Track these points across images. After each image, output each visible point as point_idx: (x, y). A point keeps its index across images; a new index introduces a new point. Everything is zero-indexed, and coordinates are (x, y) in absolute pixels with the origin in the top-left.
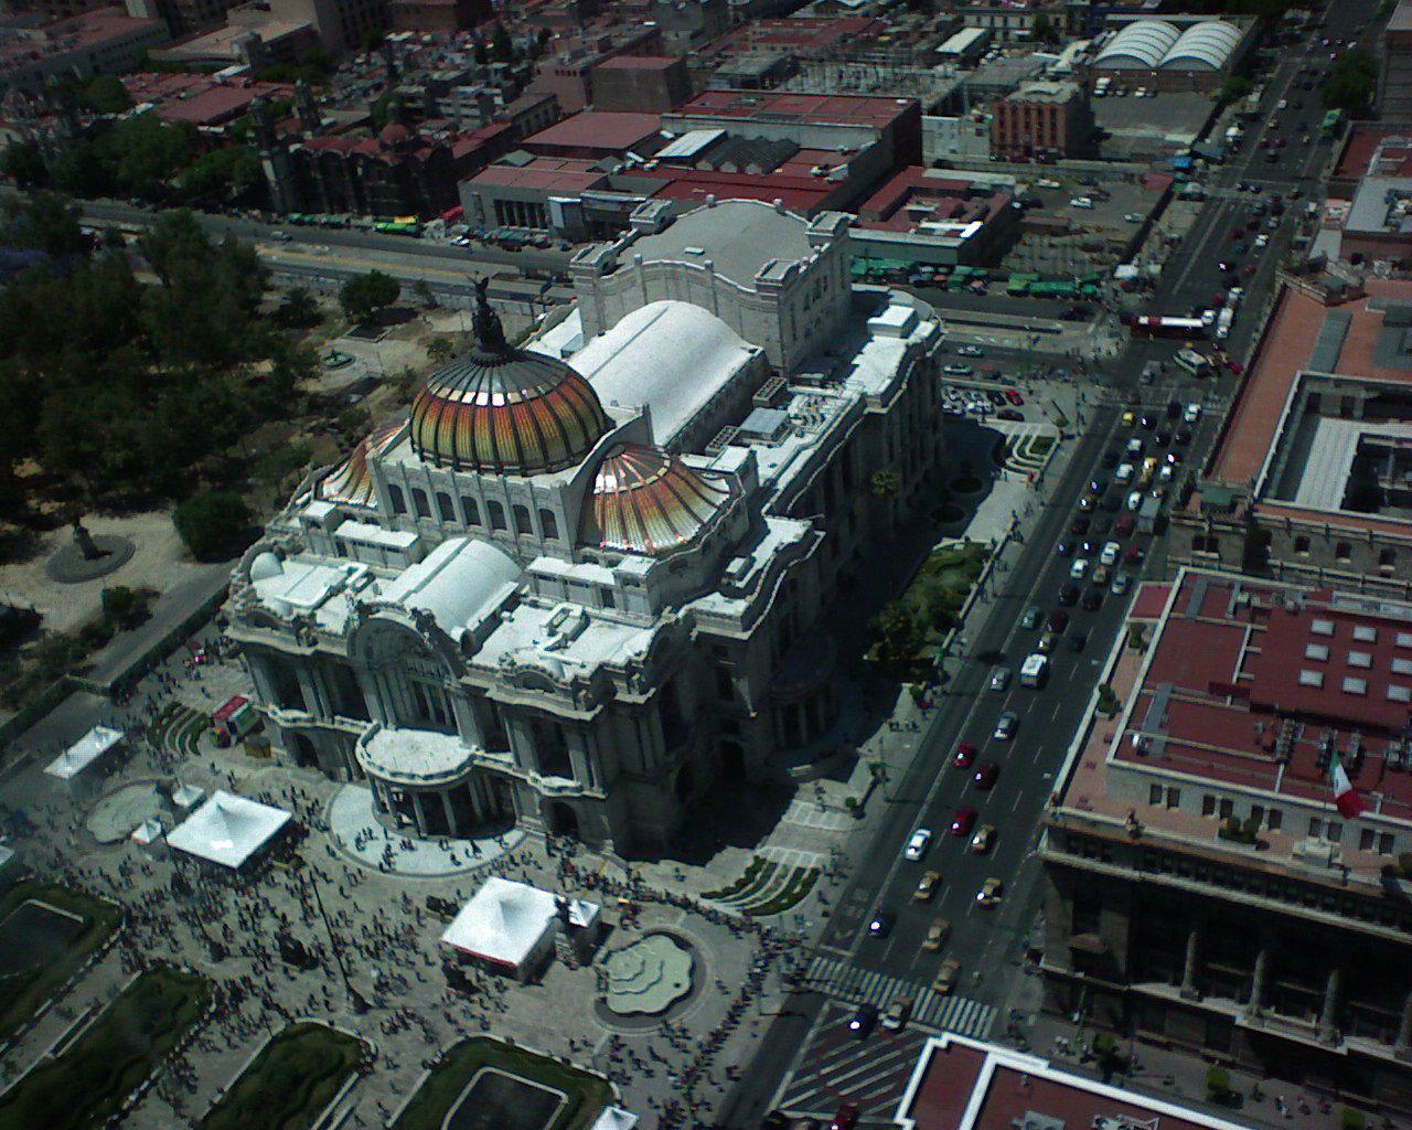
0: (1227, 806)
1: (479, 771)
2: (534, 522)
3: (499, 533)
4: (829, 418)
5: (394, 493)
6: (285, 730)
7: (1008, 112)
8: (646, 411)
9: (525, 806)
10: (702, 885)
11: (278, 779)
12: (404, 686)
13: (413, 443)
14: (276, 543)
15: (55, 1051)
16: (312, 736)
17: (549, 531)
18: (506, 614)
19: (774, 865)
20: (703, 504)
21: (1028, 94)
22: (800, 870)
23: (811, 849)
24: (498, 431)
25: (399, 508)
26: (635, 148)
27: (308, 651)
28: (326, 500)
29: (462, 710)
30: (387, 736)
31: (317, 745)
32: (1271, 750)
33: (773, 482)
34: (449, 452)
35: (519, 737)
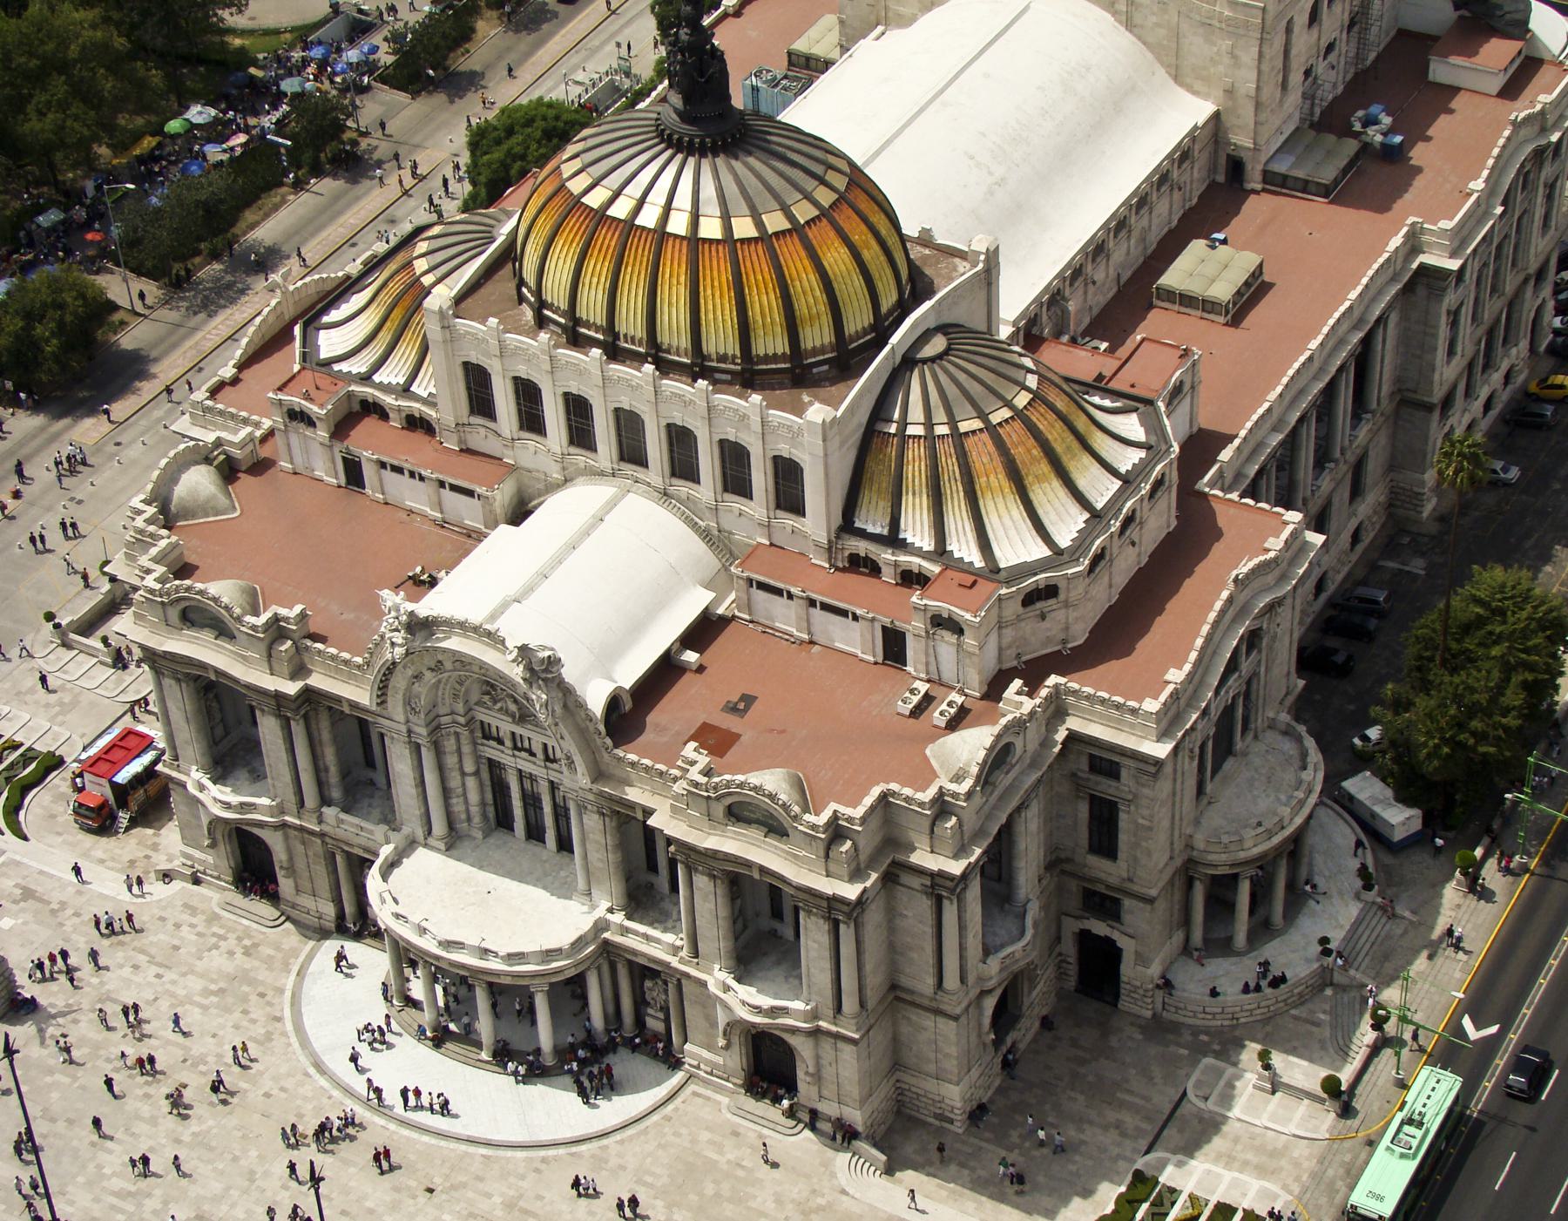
1: (609, 953)
2: (761, 478)
3: (682, 488)
6: (216, 822)
8: (992, 258)
11: (193, 911)
12: (469, 767)
14: (219, 443)
17: (789, 496)
18: (691, 657)
20: (1096, 468)
23: (1244, 1166)
24: (706, 293)
25: (481, 403)
27: (291, 688)
29: (590, 831)
34: (599, 318)
35: (705, 901)
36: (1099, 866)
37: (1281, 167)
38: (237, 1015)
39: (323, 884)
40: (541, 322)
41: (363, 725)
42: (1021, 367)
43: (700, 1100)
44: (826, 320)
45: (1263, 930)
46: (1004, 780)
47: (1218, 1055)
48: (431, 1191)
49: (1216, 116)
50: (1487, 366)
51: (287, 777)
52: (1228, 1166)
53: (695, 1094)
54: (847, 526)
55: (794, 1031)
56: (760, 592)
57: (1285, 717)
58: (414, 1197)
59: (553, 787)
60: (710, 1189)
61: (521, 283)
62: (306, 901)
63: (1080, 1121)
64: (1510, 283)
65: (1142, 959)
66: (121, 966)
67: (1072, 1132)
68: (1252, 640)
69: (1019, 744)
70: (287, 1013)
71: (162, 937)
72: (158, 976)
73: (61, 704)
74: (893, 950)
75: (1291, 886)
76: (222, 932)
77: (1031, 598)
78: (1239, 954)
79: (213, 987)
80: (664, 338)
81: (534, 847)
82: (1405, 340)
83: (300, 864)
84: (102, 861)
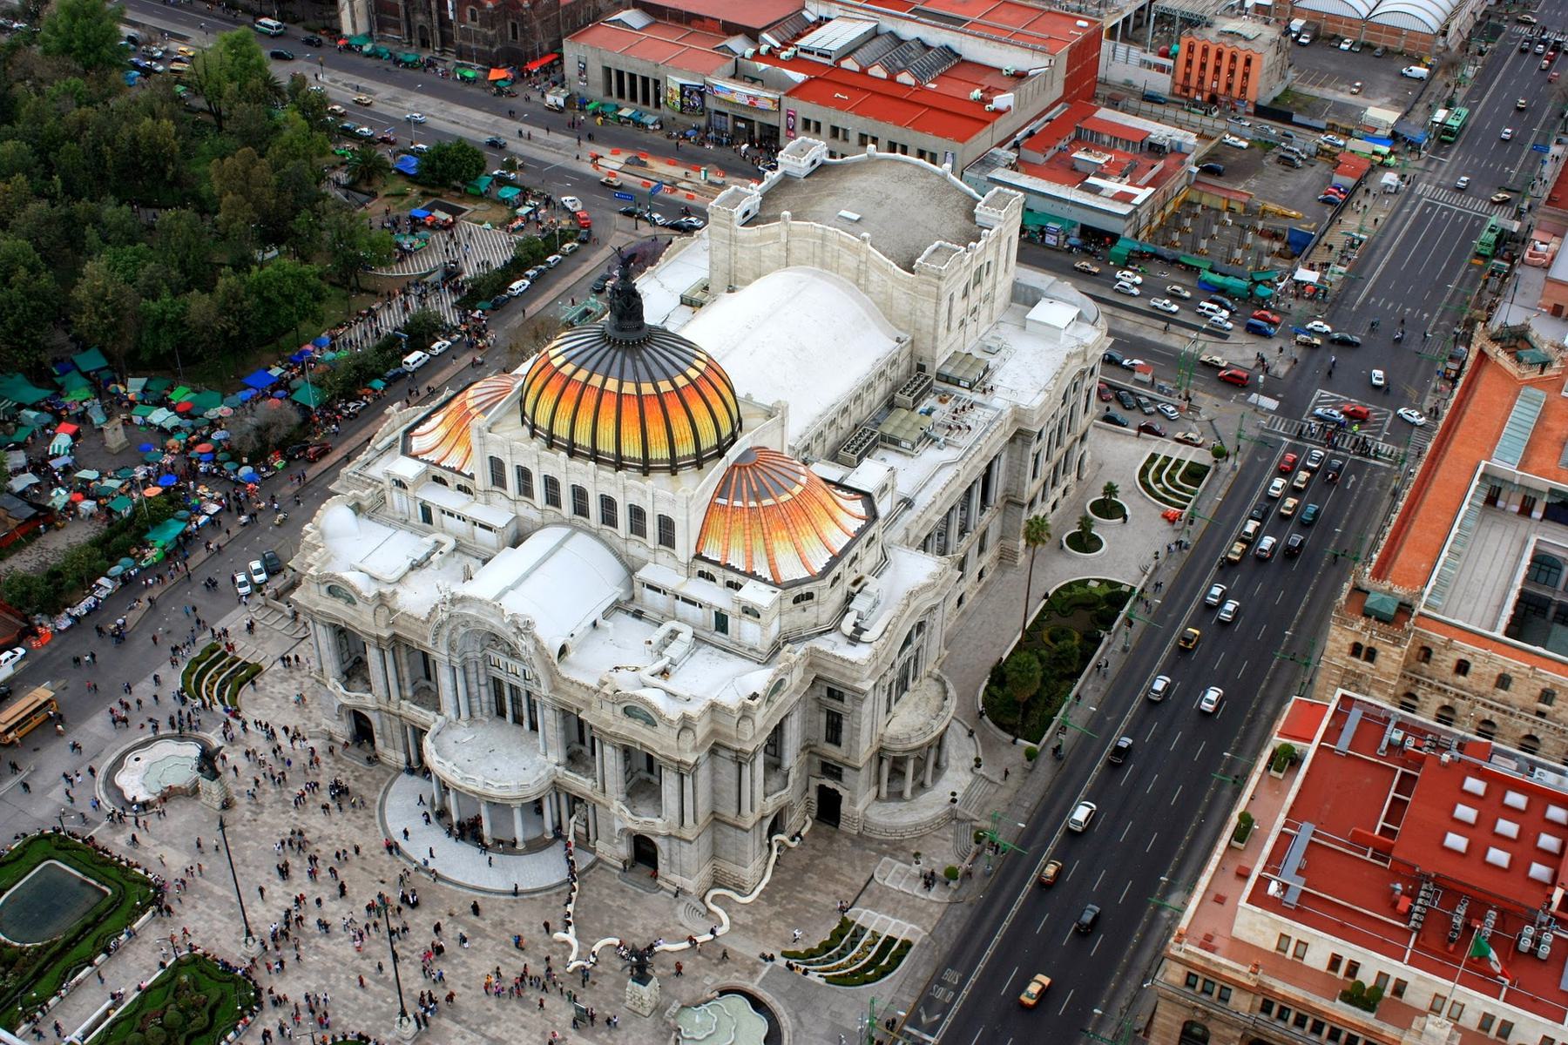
0: (1353, 967)
1: (556, 787)
2: (652, 527)
4: (977, 432)
5: (497, 466)
9: (602, 829)
10: (785, 942)
12: (483, 681)
13: (524, 414)
15: (86, 1034)
16: (374, 718)
18: (609, 624)
19: (864, 929)
20: (837, 530)
21: (1223, 34)
22: (890, 941)
25: (498, 479)
28: (415, 457)
29: (548, 719)
30: (463, 734)
31: (376, 727)
32: (1406, 917)
33: (908, 503)
34: (566, 436)
35: (610, 762)
36: (831, 750)
37: (948, 370)
39: (400, 743)
41: (425, 656)
45: (921, 787)
46: (778, 700)
47: (892, 856)
49: (912, 342)
50: (1054, 484)
51: (382, 683)
52: (894, 916)
54: (699, 557)
55: (657, 835)
57: (936, 671)
59: (529, 694)
60: (606, 922)
61: (524, 414)
62: (390, 753)
63: (815, 890)
64: (1067, 440)
65: (853, 802)
67: (809, 896)
68: (920, 626)
69: (788, 679)
74: (715, 792)
75: (937, 765)
77: (797, 600)
80: (600, 447)
81: (516, 728)
82: (1010, 468)
83: (388, 732)
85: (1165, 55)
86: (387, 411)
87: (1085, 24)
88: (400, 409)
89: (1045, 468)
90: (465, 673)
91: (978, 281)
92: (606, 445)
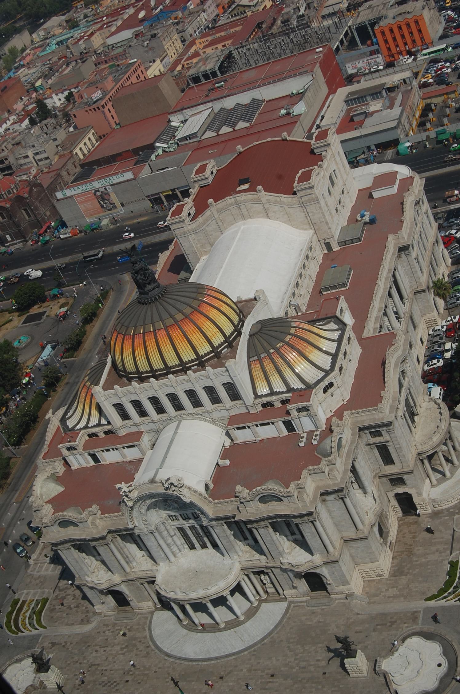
2: (223, 393)
7: (387, 33)
11: (107, 626)
25: (125, 416)
26: (158, 139)
38: (135, 651)
40: (130, 380)
42: (288, 321)
43: (297, 608)
44: (219, 334)
46: (344, 451)
48: (221, 678)
53: (294, 607)
54: (257, 396)
55: (316, 567)
56: (239, 431)
58: (217, 682)
65: (420, 494)
66: (92, 653)
68: (403, 372)
70: (151, 643)
71: (100, 638)
72: (105, 651)
73: (41, 582)
76: (119, 628)
77: (325, 391)
78: (449, 479)
79: (123, 646)
80: (170, 364)
84: (73, 624)
85: (372, 44)
86: (47, 417)
87: (321, 49)
88: (53, 413)
89: (425, 265)
90: (160, 533)
91: (333, 183)
92: (172, 360)
